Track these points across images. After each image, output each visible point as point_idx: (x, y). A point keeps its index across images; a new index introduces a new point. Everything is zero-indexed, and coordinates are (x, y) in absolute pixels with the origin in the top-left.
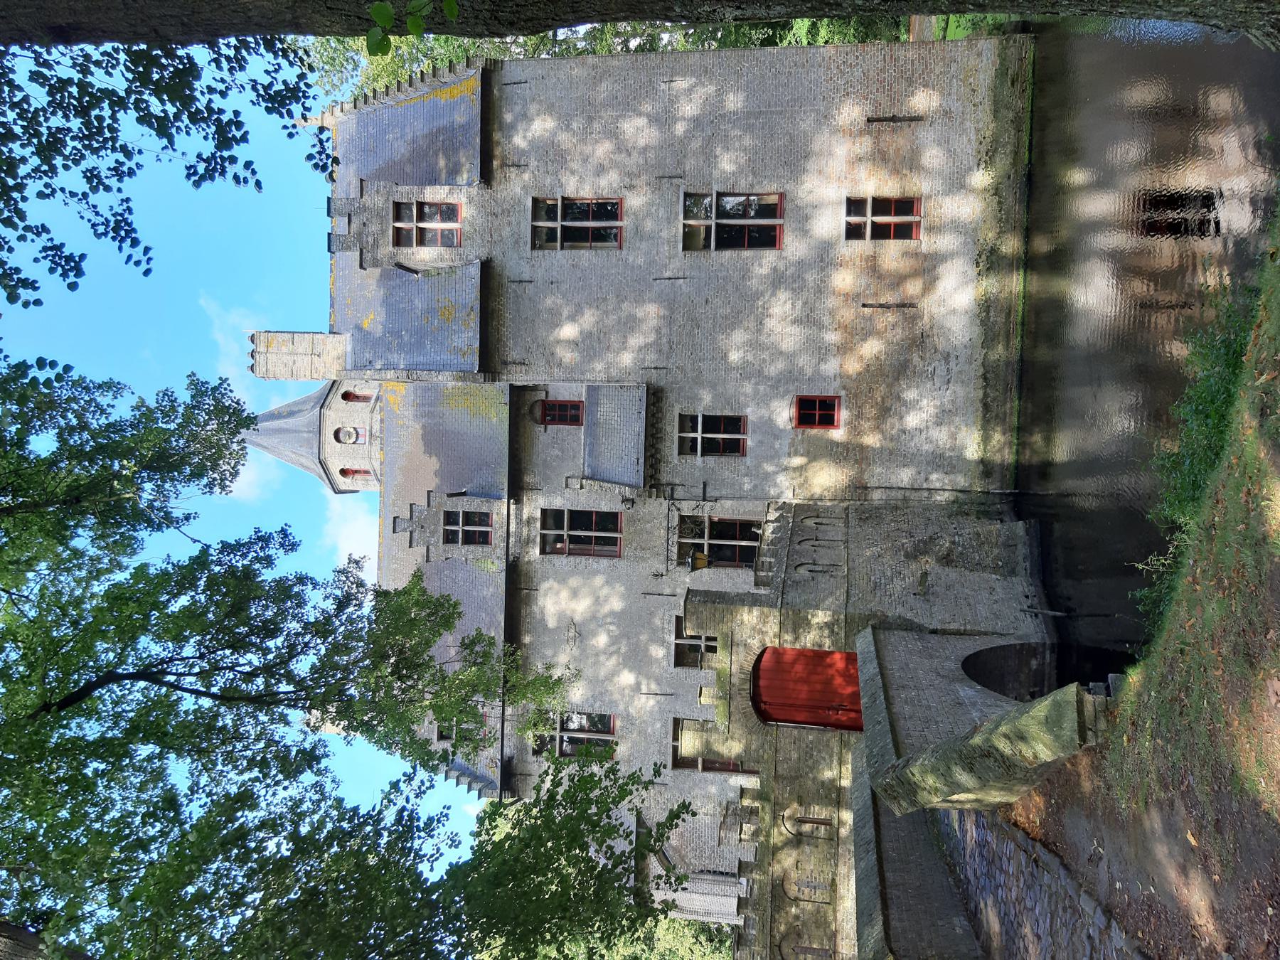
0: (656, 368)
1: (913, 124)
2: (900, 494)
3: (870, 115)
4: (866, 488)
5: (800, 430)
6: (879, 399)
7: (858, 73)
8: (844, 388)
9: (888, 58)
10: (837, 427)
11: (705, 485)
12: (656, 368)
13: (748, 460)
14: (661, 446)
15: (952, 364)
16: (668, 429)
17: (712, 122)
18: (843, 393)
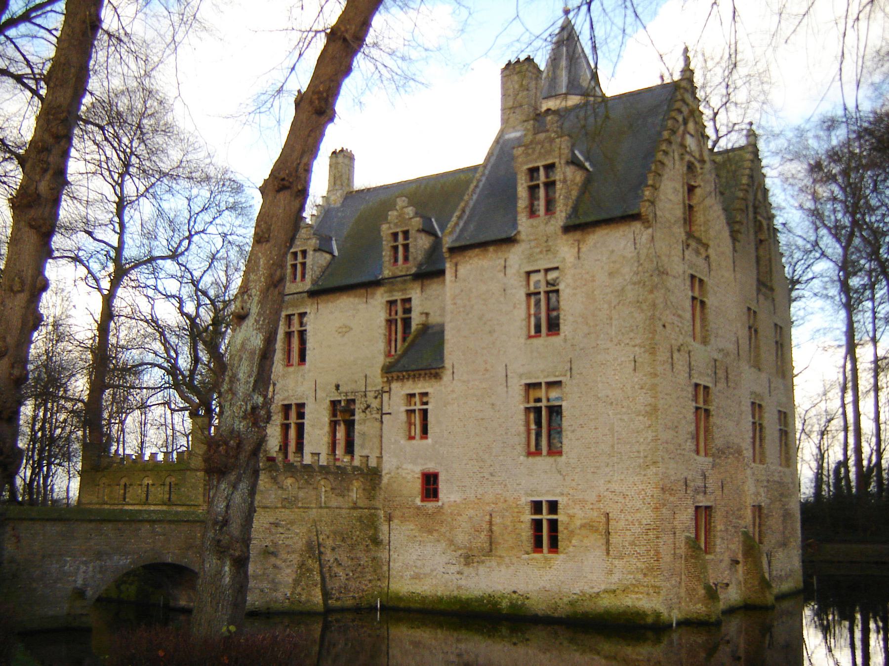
0: (453, 373)
1: (604, 547)
2: (386, 541)
3: (610, 515)
4: (390, 521)
5: (419, 475)
6: (437, 528)
7: (638, 504)
8: (443, 504)
9: (647, 527)
10: (422, 500)
11: (390, 414)
12: (453, 373)
13: (402, 442)
14: (411, 382)
15: (458, 576)
16: (420, 385)
17: (608, 397)
18: (440, 503)
